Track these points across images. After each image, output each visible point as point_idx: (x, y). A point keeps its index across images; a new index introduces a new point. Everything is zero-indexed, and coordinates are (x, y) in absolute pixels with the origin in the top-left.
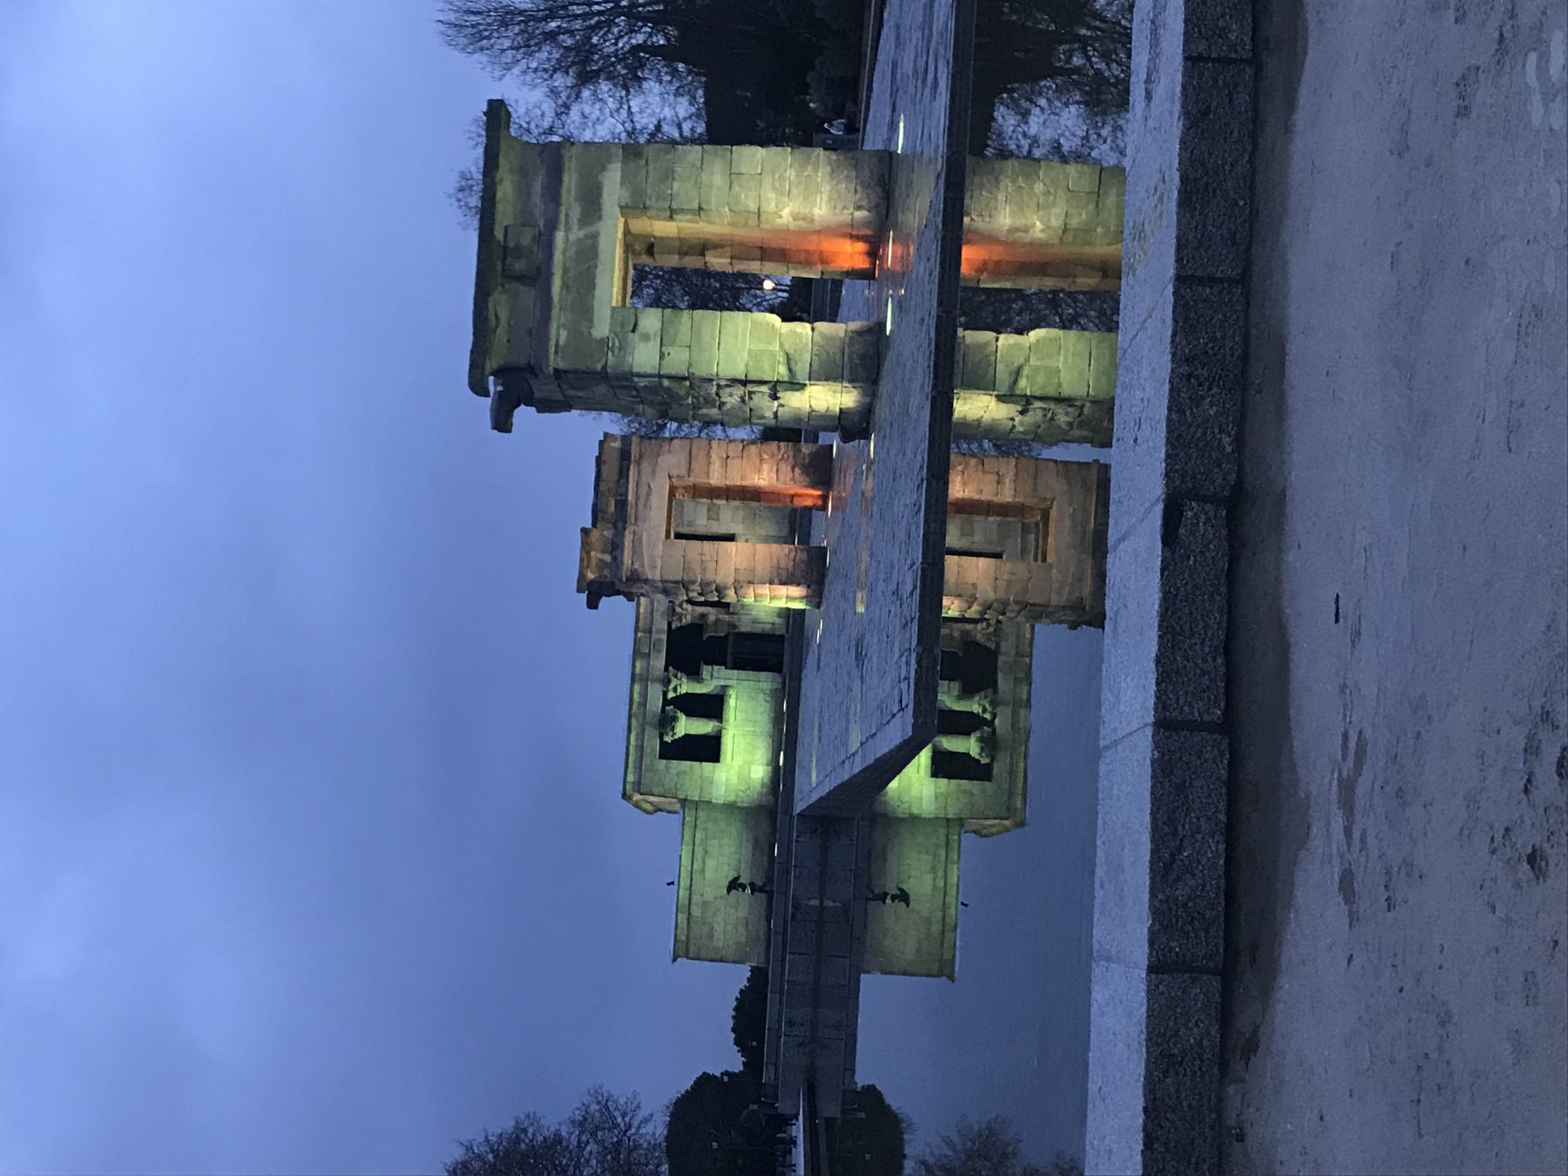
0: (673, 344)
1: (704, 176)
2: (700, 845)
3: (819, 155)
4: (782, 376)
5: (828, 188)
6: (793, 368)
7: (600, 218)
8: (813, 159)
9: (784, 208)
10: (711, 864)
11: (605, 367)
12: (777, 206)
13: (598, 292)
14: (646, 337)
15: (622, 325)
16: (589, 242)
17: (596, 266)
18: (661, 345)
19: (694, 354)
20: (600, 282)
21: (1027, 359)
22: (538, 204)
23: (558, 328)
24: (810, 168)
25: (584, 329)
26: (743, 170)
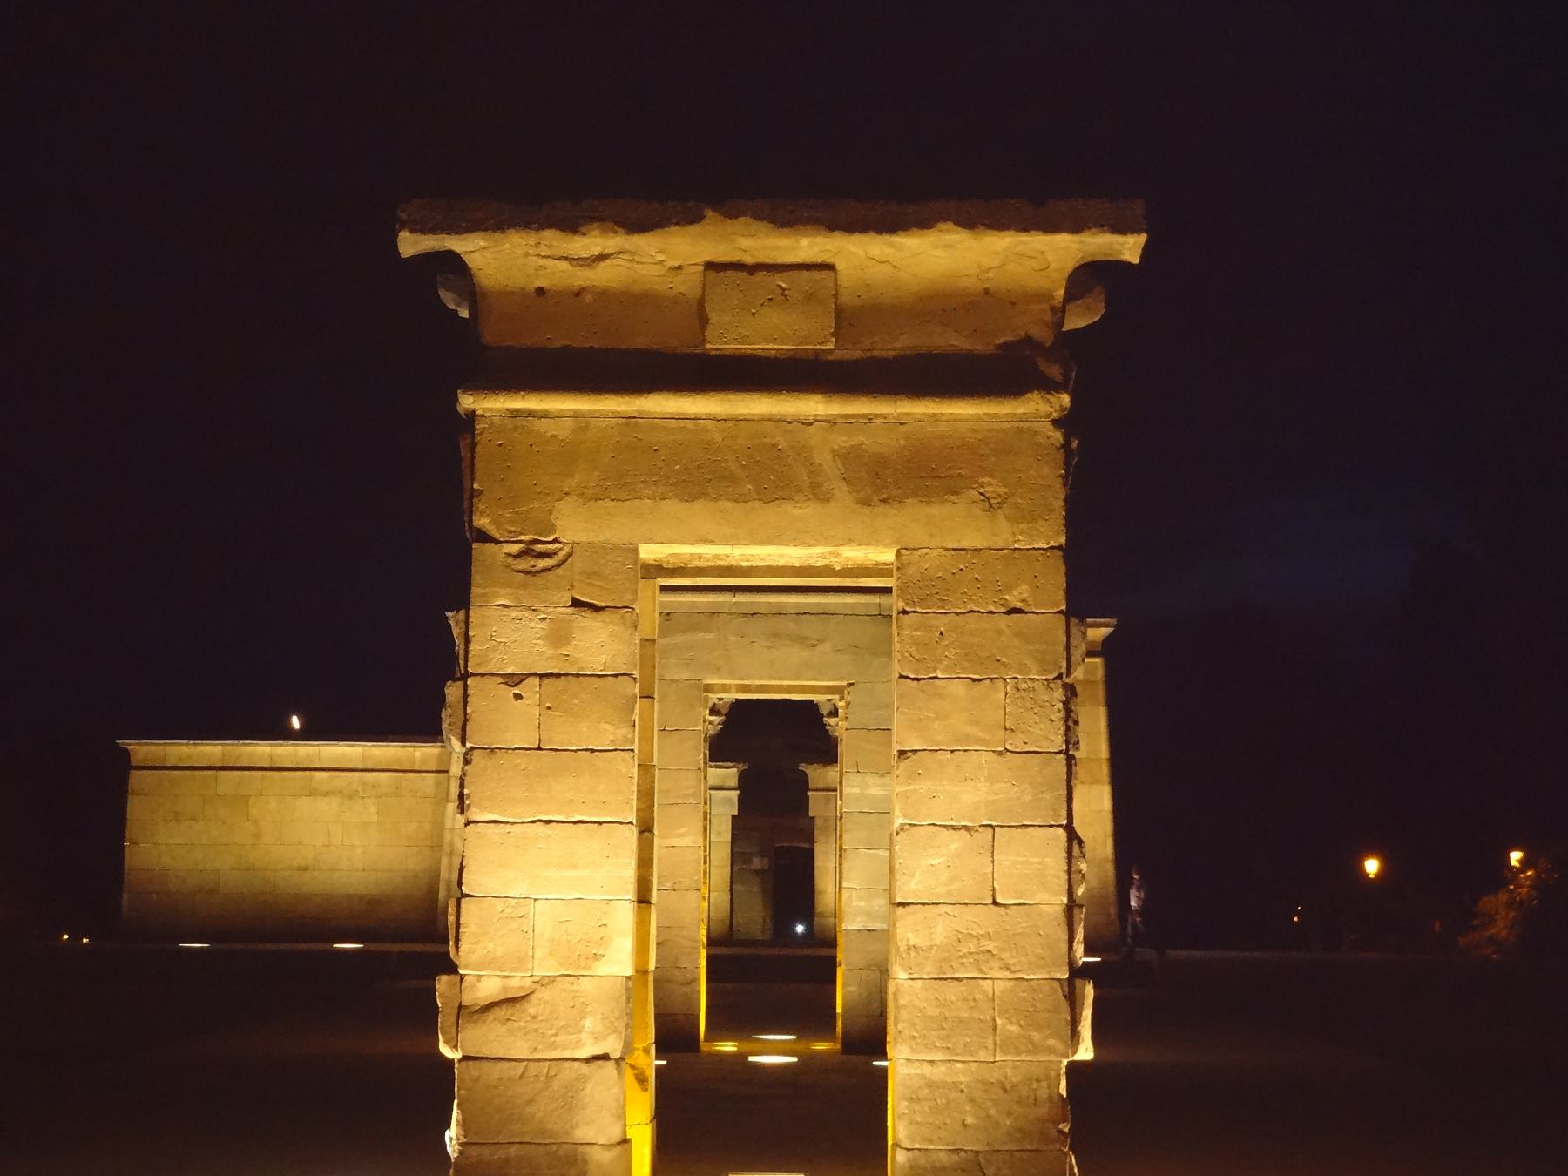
2: (364, 784)
3: (1051, 1050)
4: (472, 987)
5: (962, 1079)
6: (491, 1016)
7: (866, 502)
8: (1036, 1036)
9: (908, 969)
11: (484, 537)
13: (672, 506)
14: (559, 636)
16: (804, 479)
17: (740, 499)
18: (542, 676)
19: (520, 760)
22: (897, 345)
23: (576, 415)
25: (577, 477)
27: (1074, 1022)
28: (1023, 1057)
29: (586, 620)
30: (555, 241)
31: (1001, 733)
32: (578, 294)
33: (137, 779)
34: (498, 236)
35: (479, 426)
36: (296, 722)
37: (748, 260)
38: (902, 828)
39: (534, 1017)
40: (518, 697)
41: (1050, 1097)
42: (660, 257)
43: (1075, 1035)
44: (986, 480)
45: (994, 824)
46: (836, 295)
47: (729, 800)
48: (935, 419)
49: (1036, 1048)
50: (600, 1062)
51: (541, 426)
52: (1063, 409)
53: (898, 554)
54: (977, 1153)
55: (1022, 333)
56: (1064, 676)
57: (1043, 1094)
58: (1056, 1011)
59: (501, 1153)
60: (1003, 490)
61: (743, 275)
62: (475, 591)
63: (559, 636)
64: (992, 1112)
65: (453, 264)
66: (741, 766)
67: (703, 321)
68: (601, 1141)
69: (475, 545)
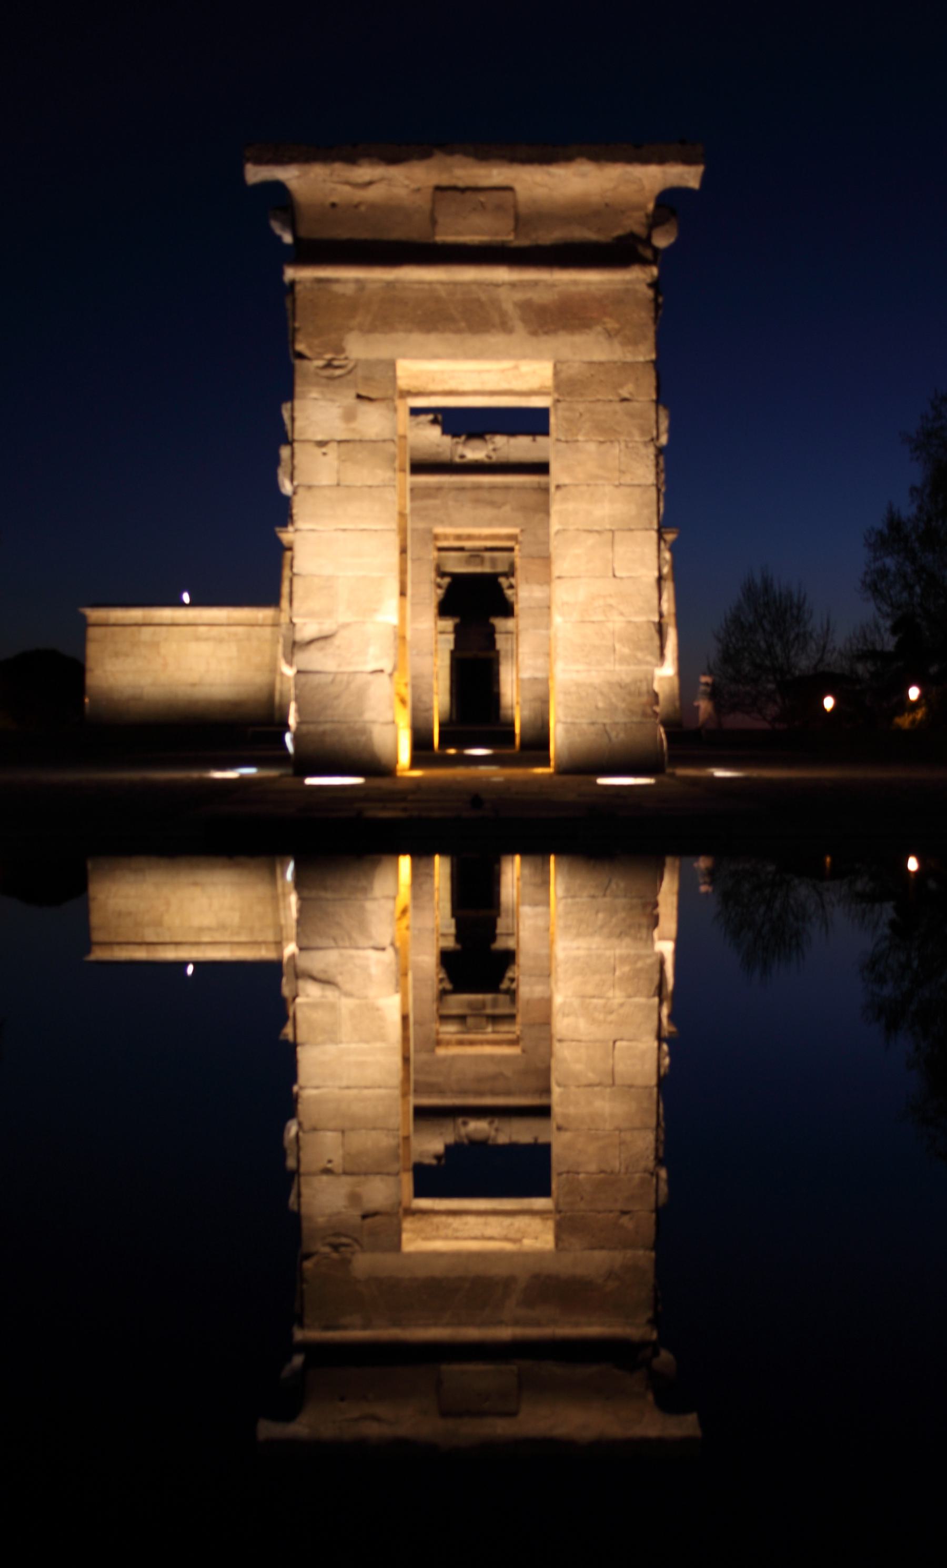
0: (342, 460)
1: (608, 489)
3: (648, 663)
6: (313, 647)
7: (534, 333)
8: (640, 655)
10: (205, 648)
12: (563, 604)
13: (417, 337)
14: (349, 416)
15: (367, 379)
16: (496, 319)
17: (458, 331)
18: (340, 442)
20: (433, 340)
21: (348, 995)
23: (358, 281)
24: (626, 651)
26: (620, 550)
27: (662, 647)
28: (633, 667)
29: (365, 407)
30: (341, 170)
31: (617, 474)
32: (357, 206)
33: (93, 632)
34: (306, 168)
35: (298, 288)
36: (186, 598)
37: (461, 184)
38: (558, 532)
39: (339, 647)
40: (324, 454)
41: (648, 692)
42: (407, 182)
43: (662, 655)
44: (606, 319)
45: (613, 528)
46: (515, 206)
47: (448, 641)
48: (575, 283)
49: (639, 662)
50: (379, 674)
51: (337, 288)
52: (652, 276)
53: (555, 366)
54: (604, 725)
55: (628, 230)
56: (655, 440)
57: (644, 688)
58: (651, 639)
59: (321, 728)
60: (617, 326)
61: (457, 195)
62: (298, 389)
63: (349, 416)
64: (614, 700)
65: (279, 188)
66: (457, 620)
67: (434, 222)
68: (381, 719)
69: (298, 363)
